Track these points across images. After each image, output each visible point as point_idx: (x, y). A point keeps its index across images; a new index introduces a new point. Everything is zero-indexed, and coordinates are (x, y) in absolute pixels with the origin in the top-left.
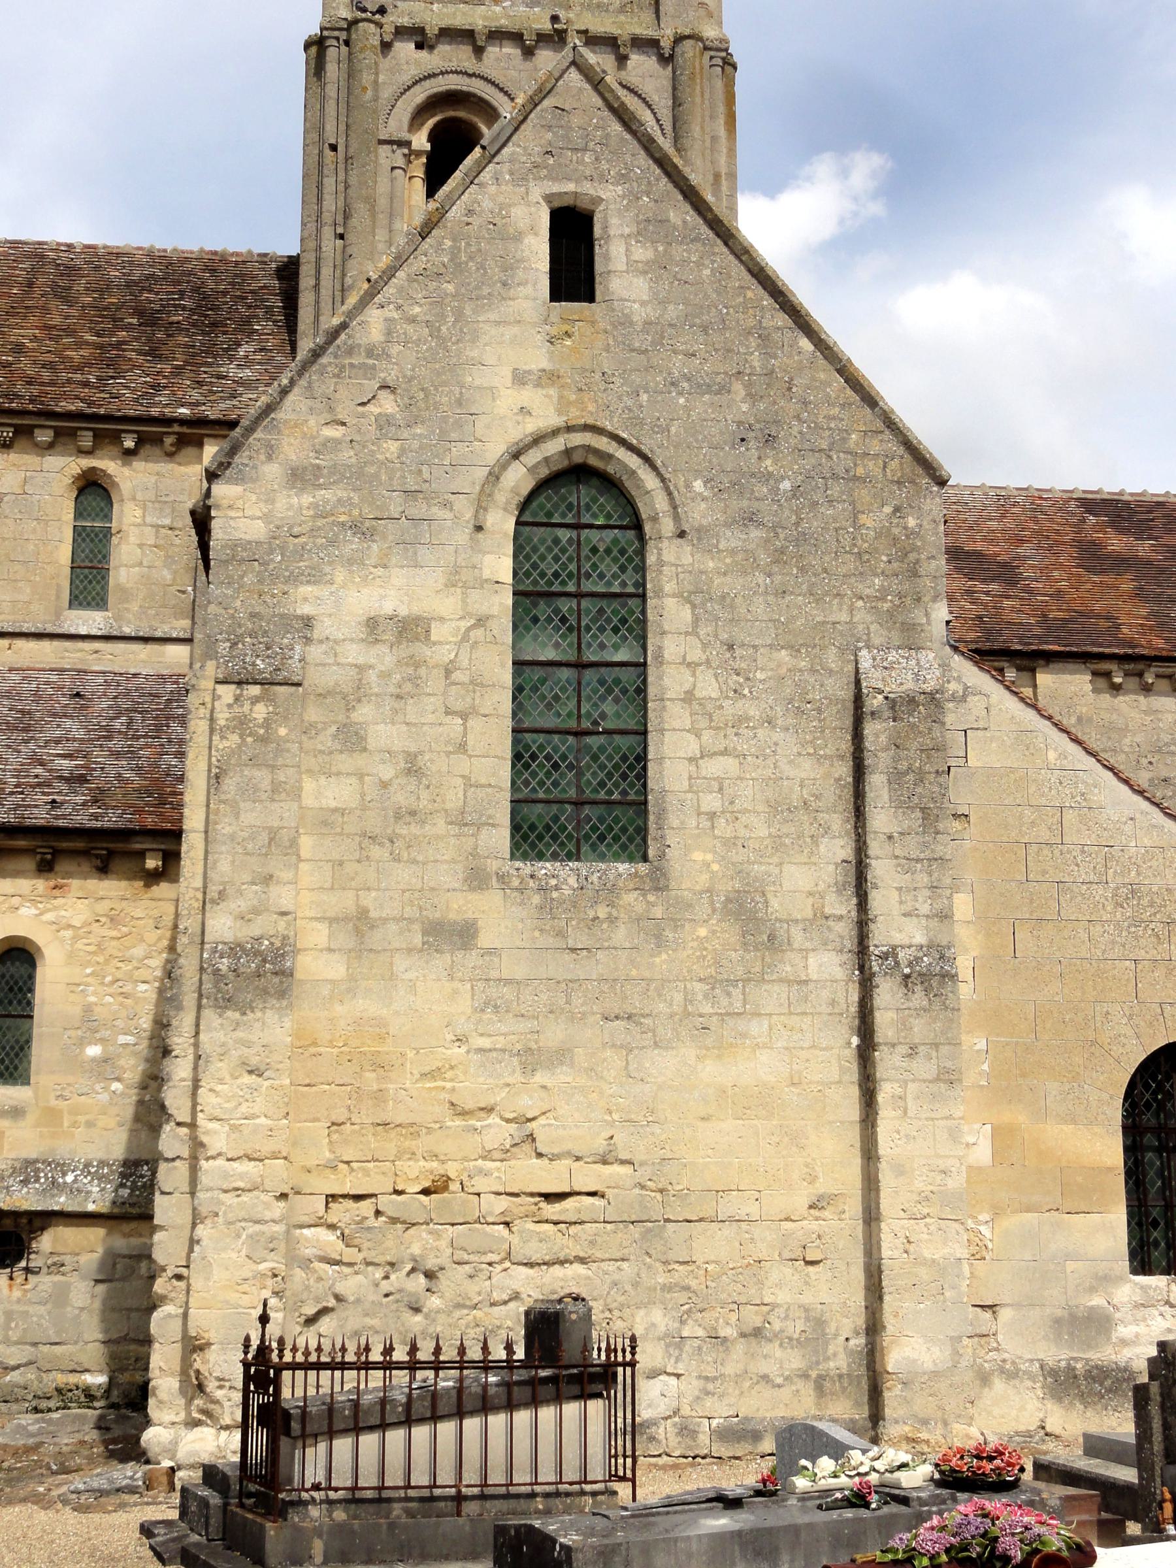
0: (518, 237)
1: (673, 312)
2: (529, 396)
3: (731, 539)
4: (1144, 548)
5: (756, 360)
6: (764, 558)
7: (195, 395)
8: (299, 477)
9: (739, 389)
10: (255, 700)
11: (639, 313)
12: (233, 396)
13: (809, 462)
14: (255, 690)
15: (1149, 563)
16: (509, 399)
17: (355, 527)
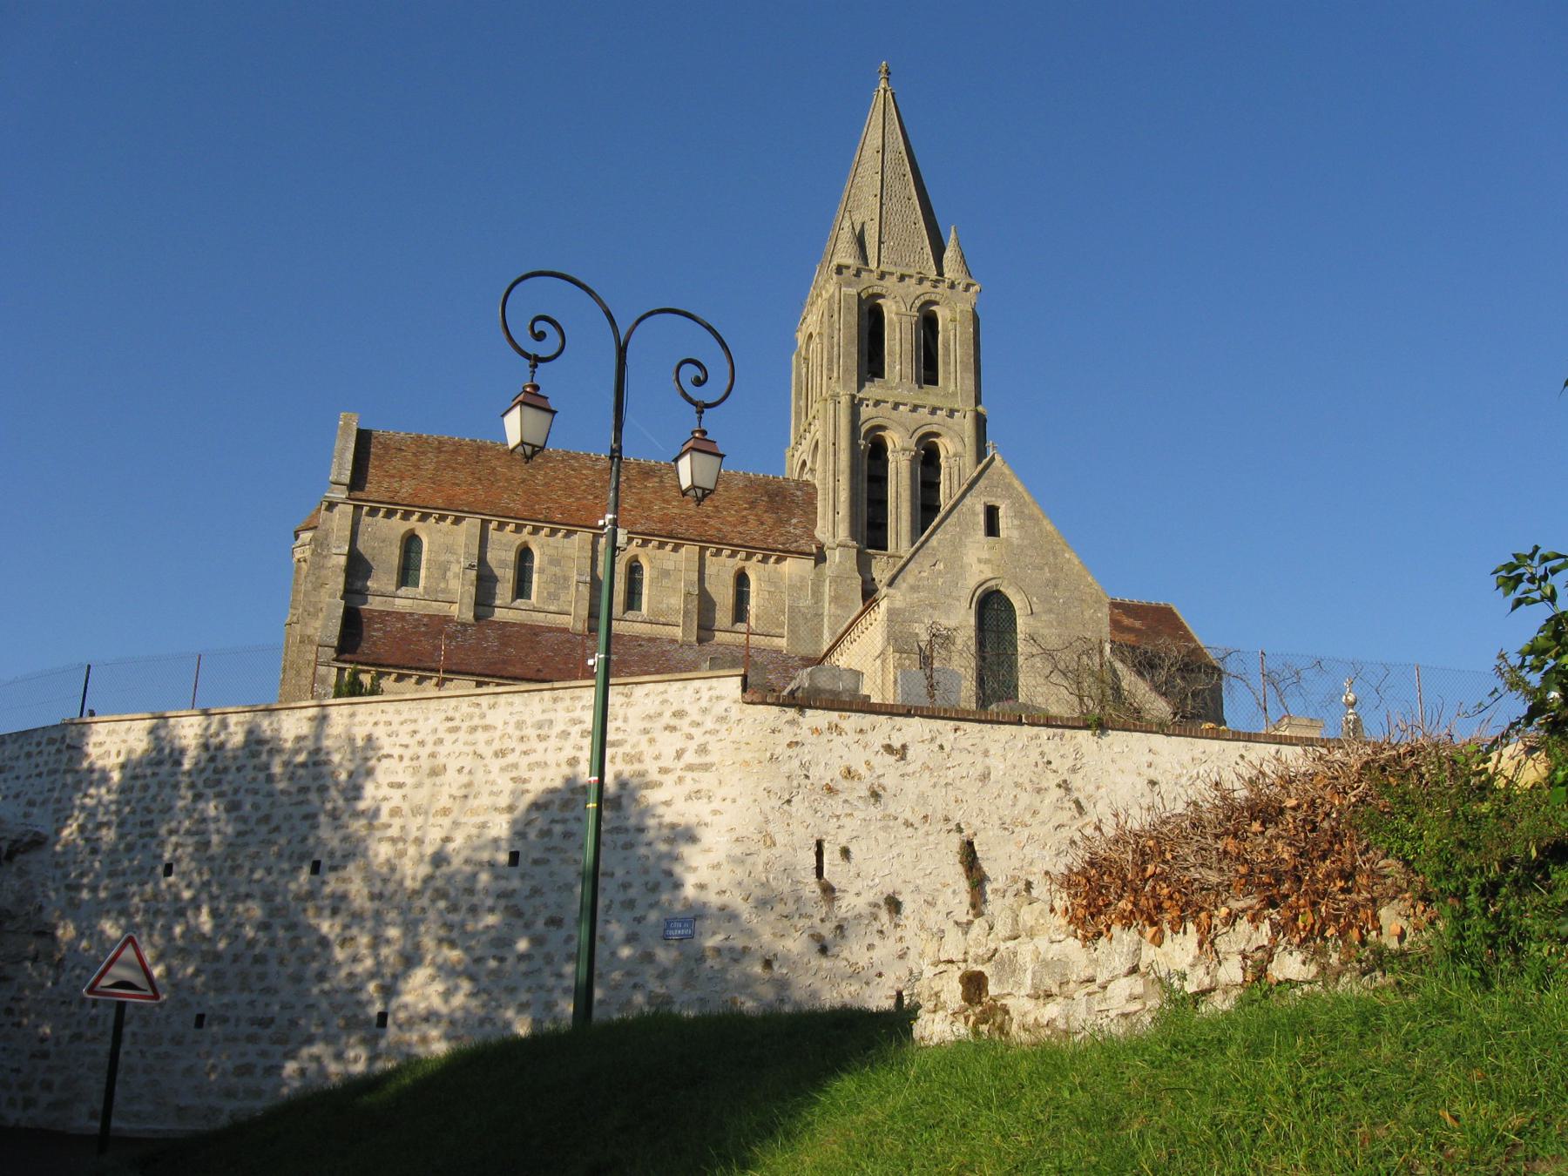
0: (978, 514)
1: (1026, 542)
2: (982, 566)
3: (1044, 617)
4: (1138, 624)
5: (1051, 559)
6: (1055, 623)
7: (781, 539)
8: (914, 588)
9: (1047, 569)
10: (905, 659)
11: (1016, 542)
12: (796, 542)
13: (1067, 594)
14: (905, 655)
15: (1140, 630)
16: (976, 567)
17: (931, 605)
